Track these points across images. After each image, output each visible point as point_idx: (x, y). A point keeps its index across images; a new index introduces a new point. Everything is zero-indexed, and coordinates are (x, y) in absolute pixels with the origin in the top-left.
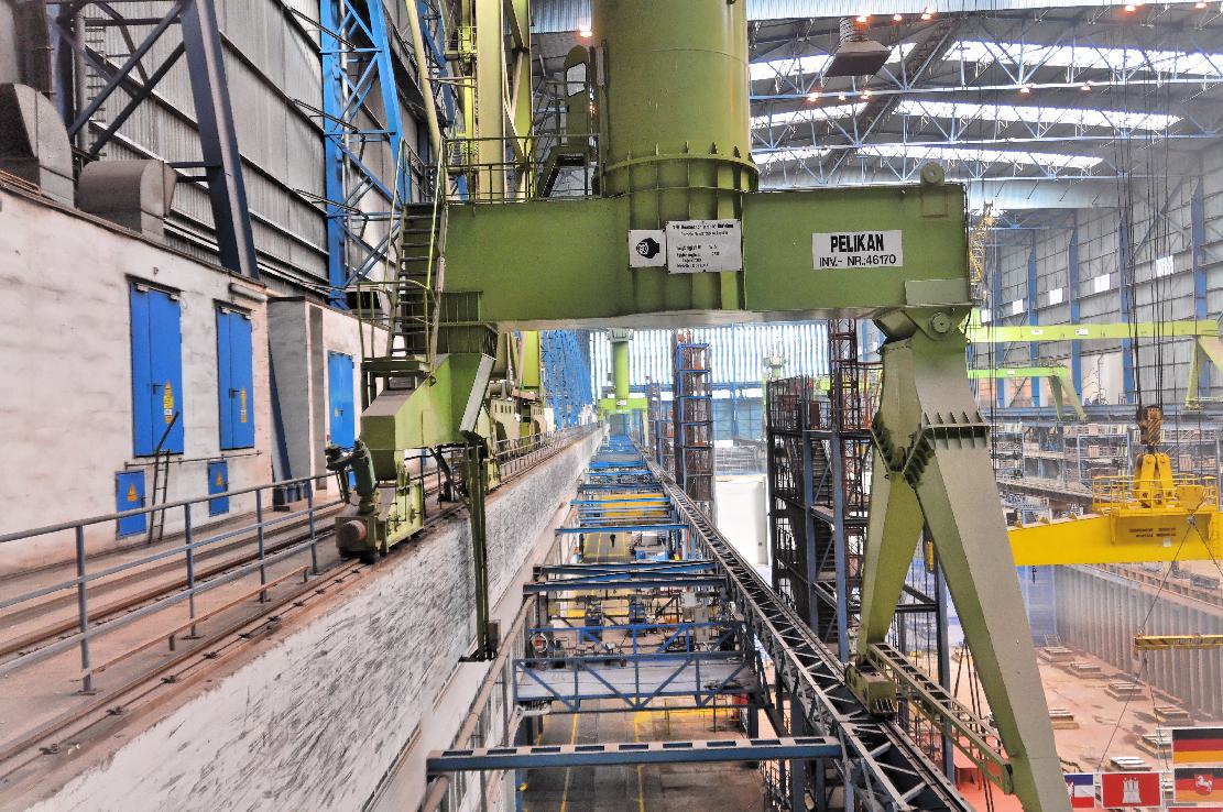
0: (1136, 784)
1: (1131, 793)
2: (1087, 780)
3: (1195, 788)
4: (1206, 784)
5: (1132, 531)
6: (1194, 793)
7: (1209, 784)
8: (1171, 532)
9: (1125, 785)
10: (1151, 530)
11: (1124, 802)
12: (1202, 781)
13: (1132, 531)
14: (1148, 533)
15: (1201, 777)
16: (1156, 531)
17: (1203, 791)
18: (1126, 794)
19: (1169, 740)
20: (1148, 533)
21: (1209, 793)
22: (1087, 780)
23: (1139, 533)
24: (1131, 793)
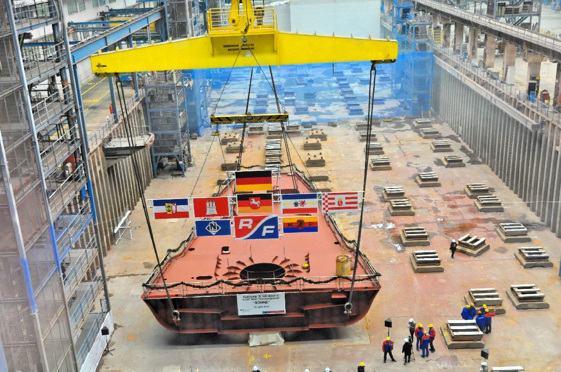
0: (214, 204)
1: (211, 209)
2: (184, 202)
3: (249, 205)
4: (256, 203)
5: (225, 46)
6: (249, 208)
7: (257, 203)
8: (250, 47)
9: (208, 204)
10: (238, 46)
11: (208, 213)
12: (254, 202)
13: (225, 46)
14: (236, 48)
15: (253, 199)
16: (239, 47)
17: (254, 207)
18: (208, 209)
19: (234, 177)
20: (236, 48)
21: (257, 208)
22: (184, 202)
23: (229, 48)
24: (211, 209)
